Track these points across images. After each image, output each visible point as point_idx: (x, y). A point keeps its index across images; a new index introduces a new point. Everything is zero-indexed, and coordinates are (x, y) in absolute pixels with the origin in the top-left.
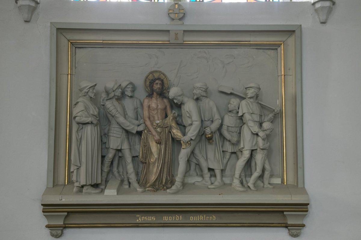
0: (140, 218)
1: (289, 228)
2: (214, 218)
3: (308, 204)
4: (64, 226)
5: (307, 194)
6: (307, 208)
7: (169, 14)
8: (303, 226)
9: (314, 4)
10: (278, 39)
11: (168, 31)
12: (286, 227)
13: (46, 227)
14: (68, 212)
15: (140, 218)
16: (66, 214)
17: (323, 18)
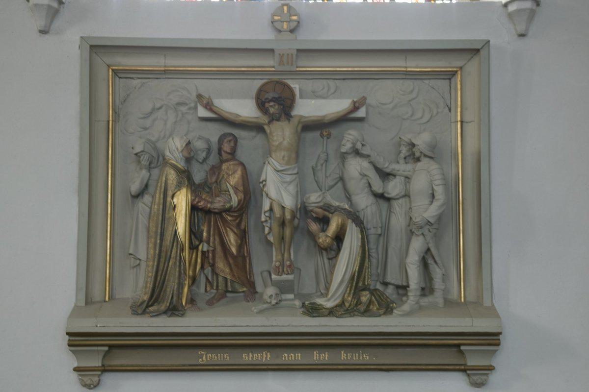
1: (469, 372)
3: (499, 334)
4: (103, 368)
5: (498, 316)
6: (499, 339)
7: (272, 22)
8: (491, 368)
9: (506, 5)
10: (453, 62)
12: (464, 371)
16: (106, 348)
17: (521, 28)
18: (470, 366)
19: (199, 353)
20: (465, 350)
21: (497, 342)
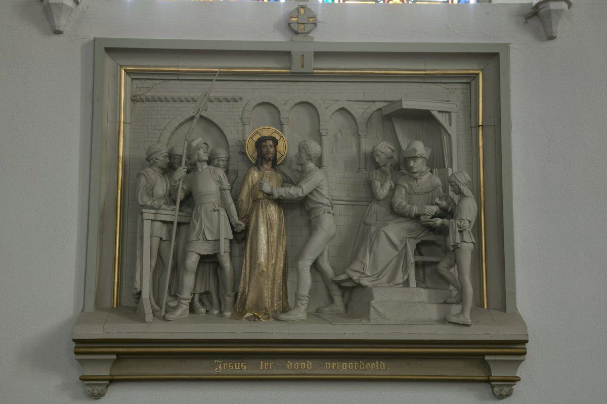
0: (220, 365)
1: (493, 383)
2: (309, 365)
3: (527, 341)
6: (525, 348)
7: (289, 24)
8: (518, 379)
11: (288, 54)
12: (488, 381)
13: (81, 379)
14: (118, 354)
15: (220, 365)
16: (114, 357)
18: (494, 376)
19: (215, 362)
20: (488, 360)
21: (522, 351)
